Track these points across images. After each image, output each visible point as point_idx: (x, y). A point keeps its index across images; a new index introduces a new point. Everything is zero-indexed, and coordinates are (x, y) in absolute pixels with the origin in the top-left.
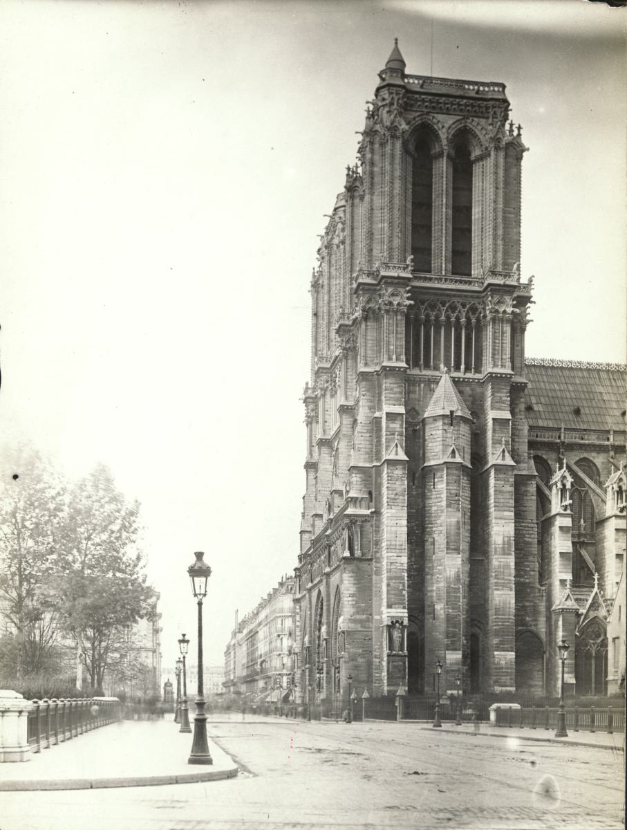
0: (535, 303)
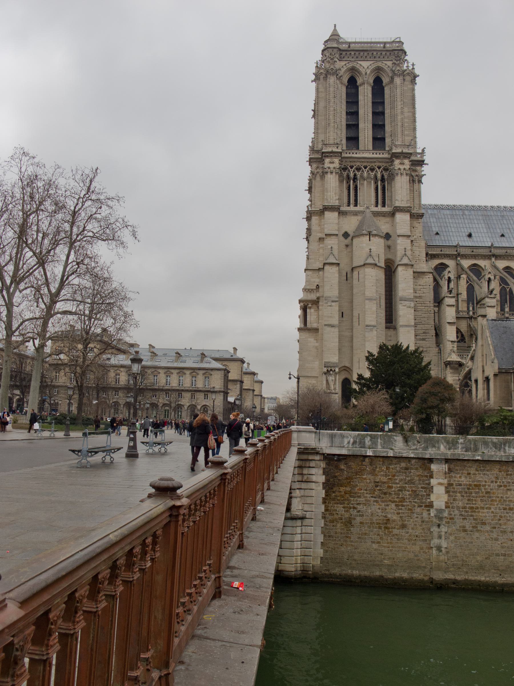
0: (427, 164)
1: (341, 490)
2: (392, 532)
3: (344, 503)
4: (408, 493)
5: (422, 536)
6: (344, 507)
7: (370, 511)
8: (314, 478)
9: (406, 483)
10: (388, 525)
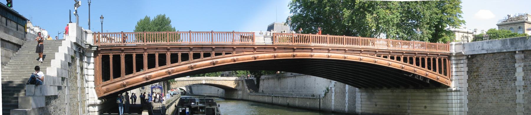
1: (475, 74)
2: (497, 96)
3: (476, 81)
4: (505, 73)
5: (512, 97)
6: (476, 84)
7: (487, 85)
8: (463, 69)
9: (504, 68)
10: (496, 93)
